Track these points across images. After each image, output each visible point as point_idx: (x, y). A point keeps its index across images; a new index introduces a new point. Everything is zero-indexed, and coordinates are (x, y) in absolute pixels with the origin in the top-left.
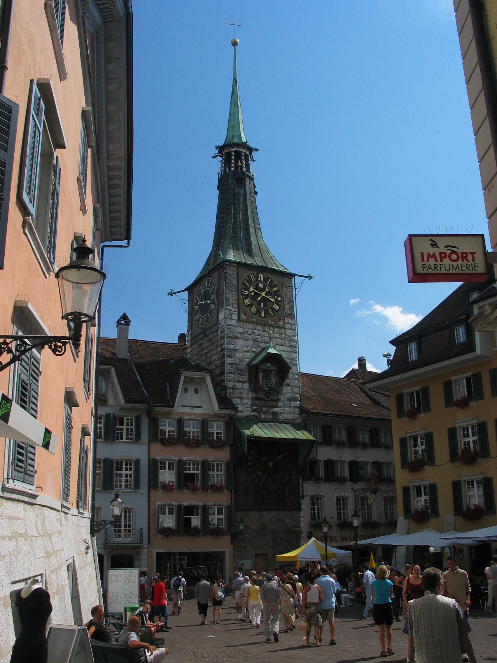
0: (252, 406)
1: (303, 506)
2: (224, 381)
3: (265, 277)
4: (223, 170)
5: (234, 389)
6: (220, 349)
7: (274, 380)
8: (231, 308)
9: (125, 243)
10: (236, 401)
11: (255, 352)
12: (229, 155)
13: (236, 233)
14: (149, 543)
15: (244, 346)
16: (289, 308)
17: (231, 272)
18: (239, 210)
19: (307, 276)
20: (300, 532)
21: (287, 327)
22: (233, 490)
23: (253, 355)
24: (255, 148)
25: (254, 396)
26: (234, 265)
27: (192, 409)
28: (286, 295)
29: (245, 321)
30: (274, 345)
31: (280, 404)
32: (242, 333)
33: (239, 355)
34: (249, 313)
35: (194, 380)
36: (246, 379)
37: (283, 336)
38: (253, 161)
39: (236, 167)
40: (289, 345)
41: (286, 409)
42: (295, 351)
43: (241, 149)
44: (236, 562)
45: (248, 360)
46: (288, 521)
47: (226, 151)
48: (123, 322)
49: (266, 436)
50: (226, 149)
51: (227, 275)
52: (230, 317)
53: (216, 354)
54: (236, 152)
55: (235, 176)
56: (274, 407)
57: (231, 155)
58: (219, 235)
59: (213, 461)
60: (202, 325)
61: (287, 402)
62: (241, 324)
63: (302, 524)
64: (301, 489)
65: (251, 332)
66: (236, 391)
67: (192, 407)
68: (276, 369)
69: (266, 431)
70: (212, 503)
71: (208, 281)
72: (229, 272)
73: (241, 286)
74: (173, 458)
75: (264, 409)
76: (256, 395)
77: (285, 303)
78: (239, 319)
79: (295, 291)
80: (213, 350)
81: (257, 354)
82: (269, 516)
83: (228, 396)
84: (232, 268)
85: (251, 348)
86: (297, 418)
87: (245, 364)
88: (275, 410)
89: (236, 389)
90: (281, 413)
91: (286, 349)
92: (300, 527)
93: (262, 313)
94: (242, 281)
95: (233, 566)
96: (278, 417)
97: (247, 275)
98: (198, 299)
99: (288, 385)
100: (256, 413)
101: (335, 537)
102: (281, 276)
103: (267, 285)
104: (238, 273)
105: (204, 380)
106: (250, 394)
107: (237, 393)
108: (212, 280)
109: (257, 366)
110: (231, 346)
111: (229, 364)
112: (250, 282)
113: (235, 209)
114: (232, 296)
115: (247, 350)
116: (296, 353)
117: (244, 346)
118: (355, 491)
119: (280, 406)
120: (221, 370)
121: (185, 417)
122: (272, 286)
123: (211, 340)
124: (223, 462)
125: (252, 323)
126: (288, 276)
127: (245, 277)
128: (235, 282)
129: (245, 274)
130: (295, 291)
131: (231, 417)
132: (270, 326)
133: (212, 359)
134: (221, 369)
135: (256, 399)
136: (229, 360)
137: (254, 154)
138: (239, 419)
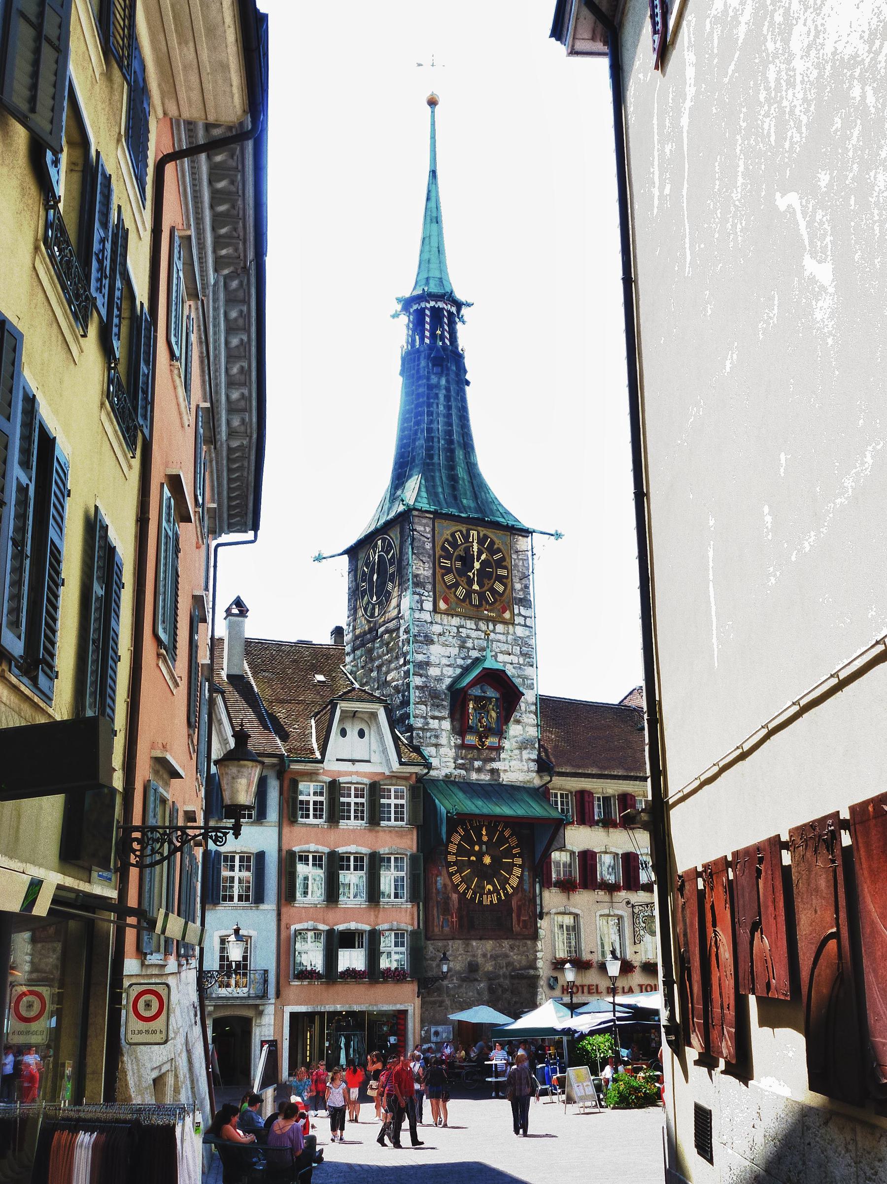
0: (455, 760)
1: (541, 932)
2: (407, 716)
3: (481, 535)
4: (410, 341)
5: (425, 731)
6: (402, 661)
7: (494, 714)
8: (422, 591)
9: (250, 535)
10: (428, 751)
11: (461, 666)
12: (420, 313)
13: (431, 457)
14: (278, 995)
15: (443, 656)
16: (522, 590)
17: (422, 529)
18: (438, 415)
19: (553, 532)
20: (537, 977)
21: (518, 620)
22: (421, 904)
23: (458, 671)
25: (459, 741)
26: (428, 515)
28: (516, 565)
29: (445, 614)
30: (493, 653)
31: (502, 756)
32: (440, 635)
33: (433, 672)
34: (452, 598)
35: (357, 715)
36: (445, 713)
37: (510, 637)
38: (464, 322)
39: (433, 336)
40: (521, 652)
41: (513, 763)
43: (441, 305)
44: (426, 1028)
45: (450, 680)
46: (515, 957)
47: (415, 307)
48: (235, 611)
49: (477, 811)
51: (415, 533)
52: (419, 606)
53: (396, 668)
54: (433, 309)
55: (431, 354)
56: (493, 760)
57: (425, 315)
59: (388, 854)
60: (372, 616)
61: (517, 752)
62: (438, 618)
63: (540, 964)
64: (538, 902)
65: (456, 631)
66: (428, 734)
67: (353, 761)
68: (498, 696)
69: (479, 803)
70: (385, 926)
71: (384, 540)
72: (420, 528)
73: (439, 552)
74: (321, 848)
75: (477, 764)
76: (463, 741)
77: (514, 581)
78: (435, 610)
79: (533, 559)
80: (390, 662)
81: (466, 670)
82: (483, 948)
83: (415, 742)
84: (424, 521)
85: (455, 659)
86: (534, 779)
87: (444, 687)
88: (495, 765)
90: (505, 771)
91: (515, 659)
92: (536, 969)
93: (475, 599)
94: (440, 543)
95: (421, 1035)
96: (499, 777)
97: (449, 532)
98: (366, 570)
99: (518, 722)
100: (463, 772)
101: (597, 986)
103: (484, 550)
104: (433, 530)
105: (374, 715)
106: (452, 738)
107: (430, 738)
108: (389, 540)
109: (464, 690)
110: (420, 658)
111: (417, 687)
112: (454, 545)
114: (424, 570)
115: (448, 663)
116: (532, 666)
117: (443, 656)
118: (633, 906)
119: (504, 759)
120: (403, 698)
121: (342, 780)
122: (492, 550)
123: (388, 644)
124: (406, 855)
125: (457, 616)
127: (445, 536)
128: (428, 546)
129: (447, 530)
130: (533, 559)
131: (420, 779)
132: (488, 620)
133: (389, 678)
134: (403, 696)
135: (463, 746)
136: (418, 681)
137: (464, 311)
138: (434, 781)
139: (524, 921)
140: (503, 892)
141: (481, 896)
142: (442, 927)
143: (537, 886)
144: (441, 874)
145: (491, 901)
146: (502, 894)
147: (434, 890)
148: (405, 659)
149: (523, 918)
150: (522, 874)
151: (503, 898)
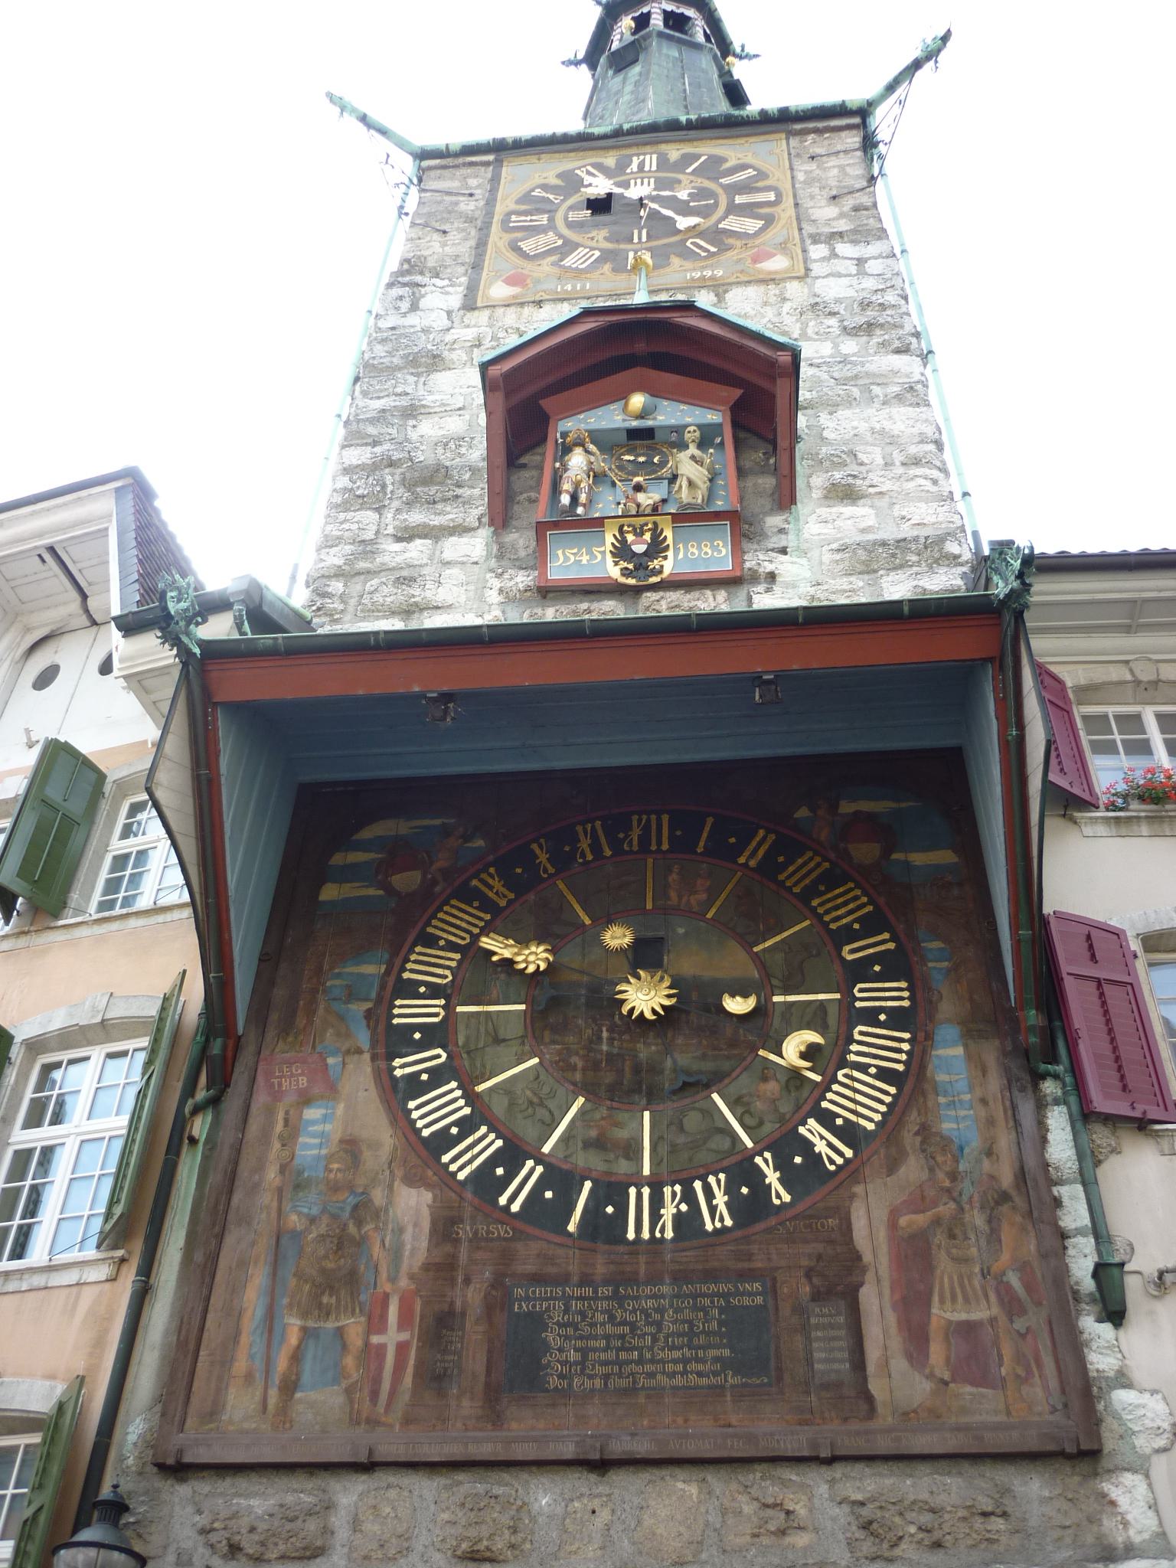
42: (897, 344)
64: (1075, 1213)
102: (783, 136)
126: (820, 125)
139: (968, 1329)
140: (782, 1165)
141: (612, 1191)
142: (290, 1387)
143: (1058, 1122)
144: (332, 1091)
145: (688, 1223)
146: (772, 1177)
147: (272, 1174)
149: (943, 1313)
150: (918, 1060)
151: (780, 1194)
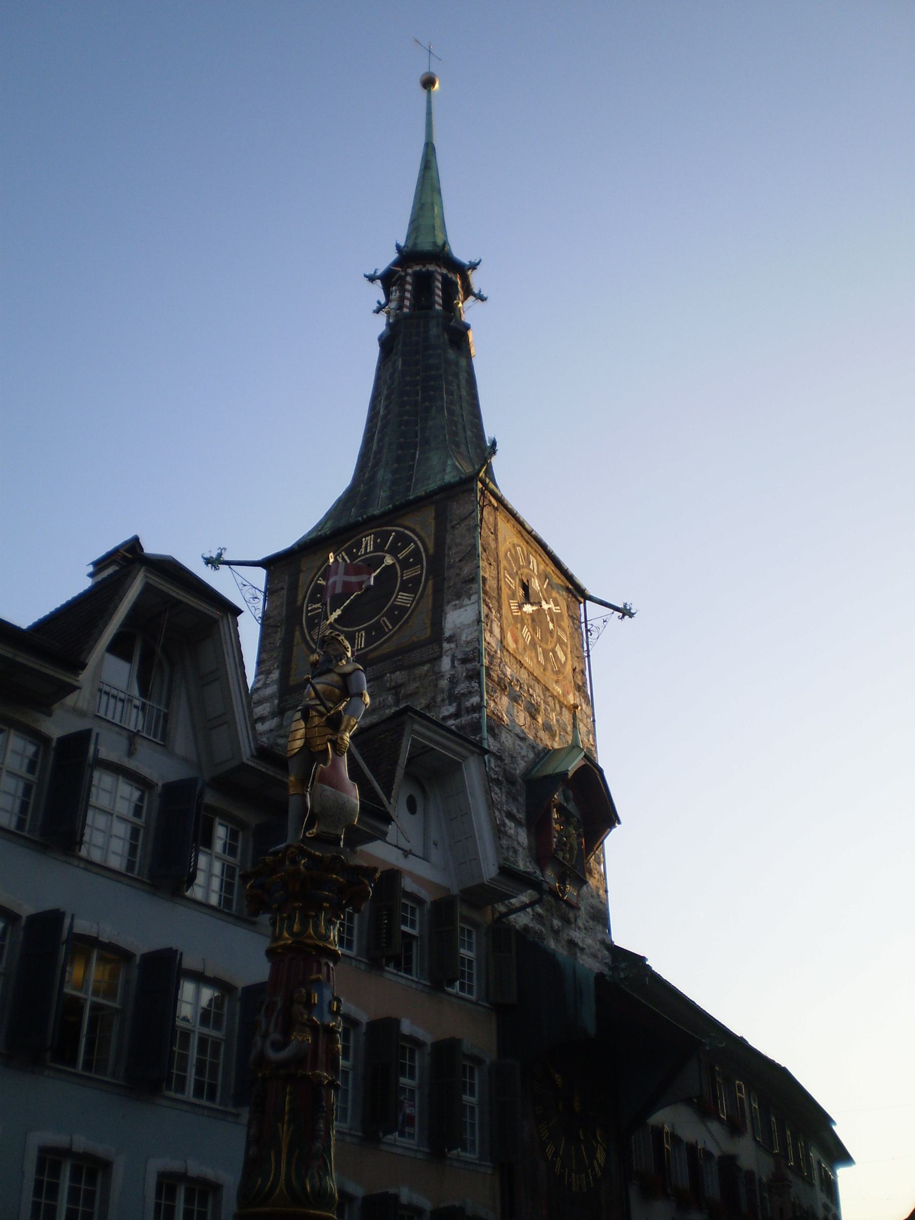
19: (621, 606)
24: (480, 291)
27: (406, 856)
47: (417, 268)
50: (416, 264)
58: (402, 440)
89: (505, 833)
113: (450, 393)
148: (459, 706)
